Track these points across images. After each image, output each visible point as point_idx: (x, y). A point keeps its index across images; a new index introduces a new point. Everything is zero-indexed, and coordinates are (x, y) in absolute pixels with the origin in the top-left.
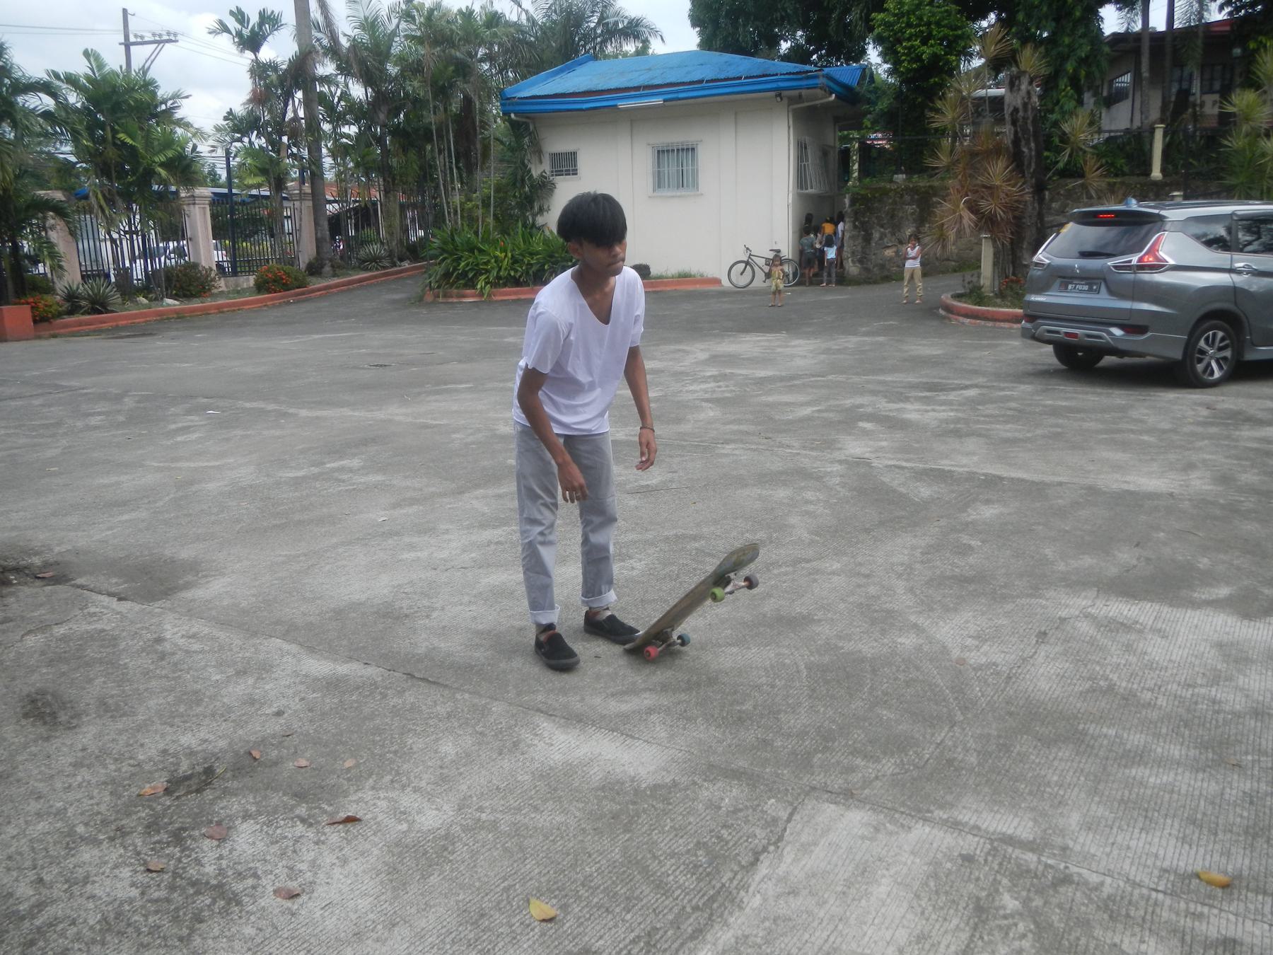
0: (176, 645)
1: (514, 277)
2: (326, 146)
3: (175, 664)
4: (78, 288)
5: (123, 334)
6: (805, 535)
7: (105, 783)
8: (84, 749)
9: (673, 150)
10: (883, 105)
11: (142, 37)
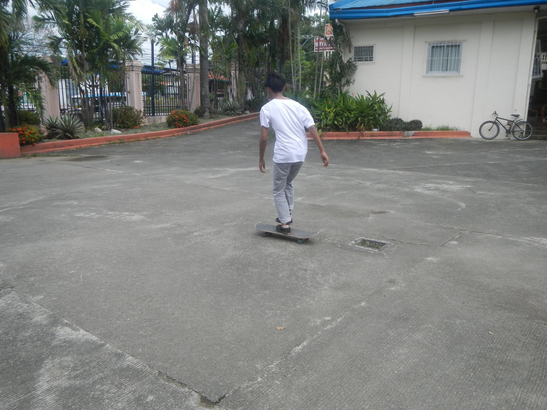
2: (209, 41)
4: (56, 121)
5: (84, 155)
9: (444, 46)
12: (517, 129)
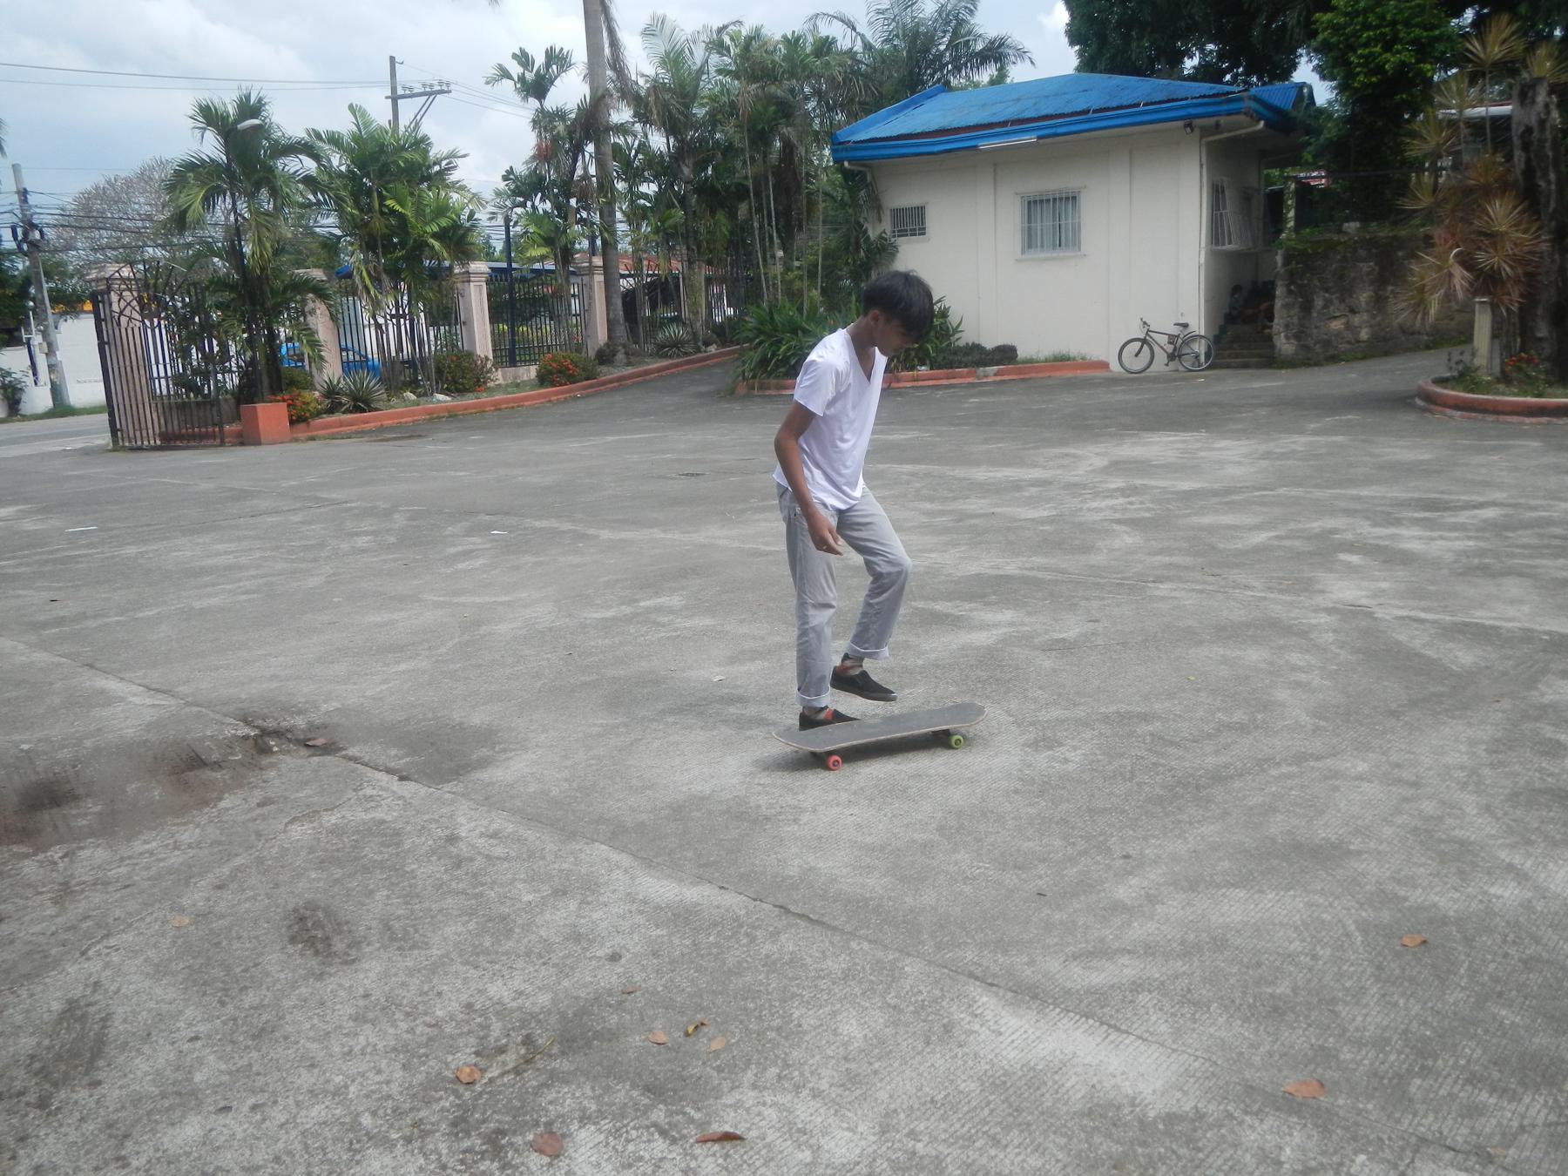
0: (473, 846)
3: (475, 875)
4: (339, 382)
5: (389, 436)
6: (1304, 719)
7: (394, 1049)
8: (366, 996)
9: (1048, 201)
10: (1330, 132)
11: (411, 89)
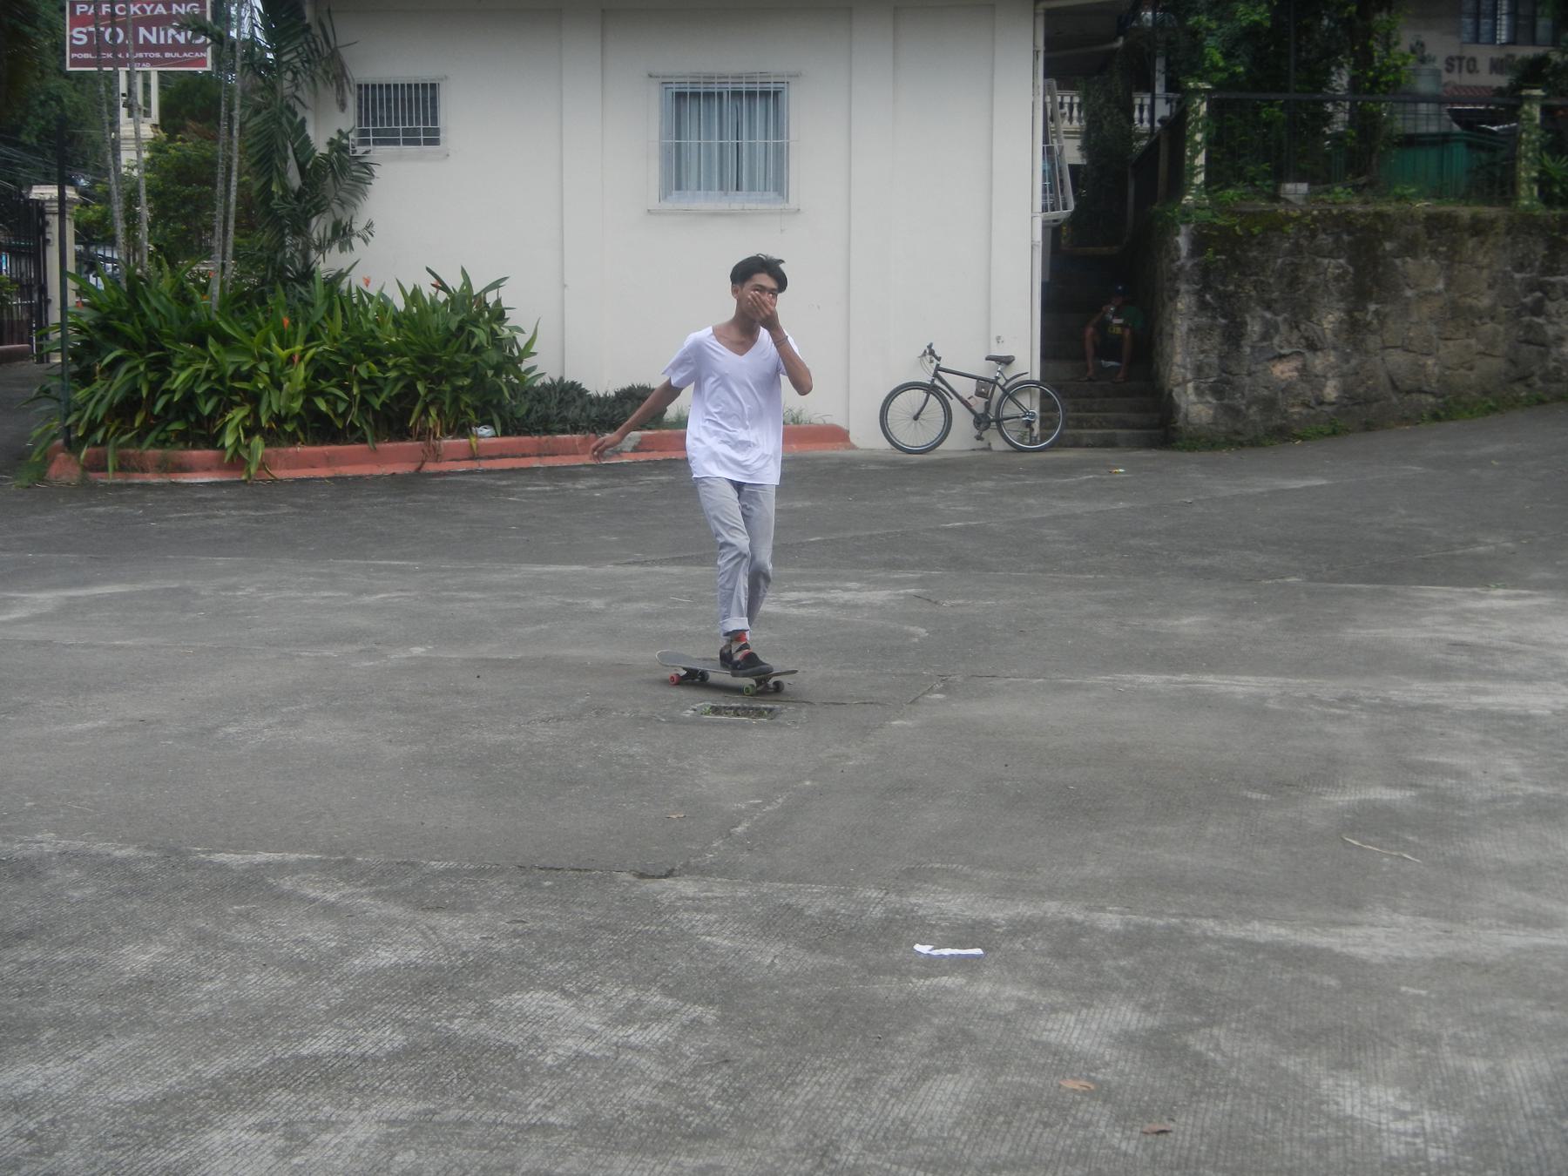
1: (320, 416)
9: (720, 95)
12: (1010, 409)
